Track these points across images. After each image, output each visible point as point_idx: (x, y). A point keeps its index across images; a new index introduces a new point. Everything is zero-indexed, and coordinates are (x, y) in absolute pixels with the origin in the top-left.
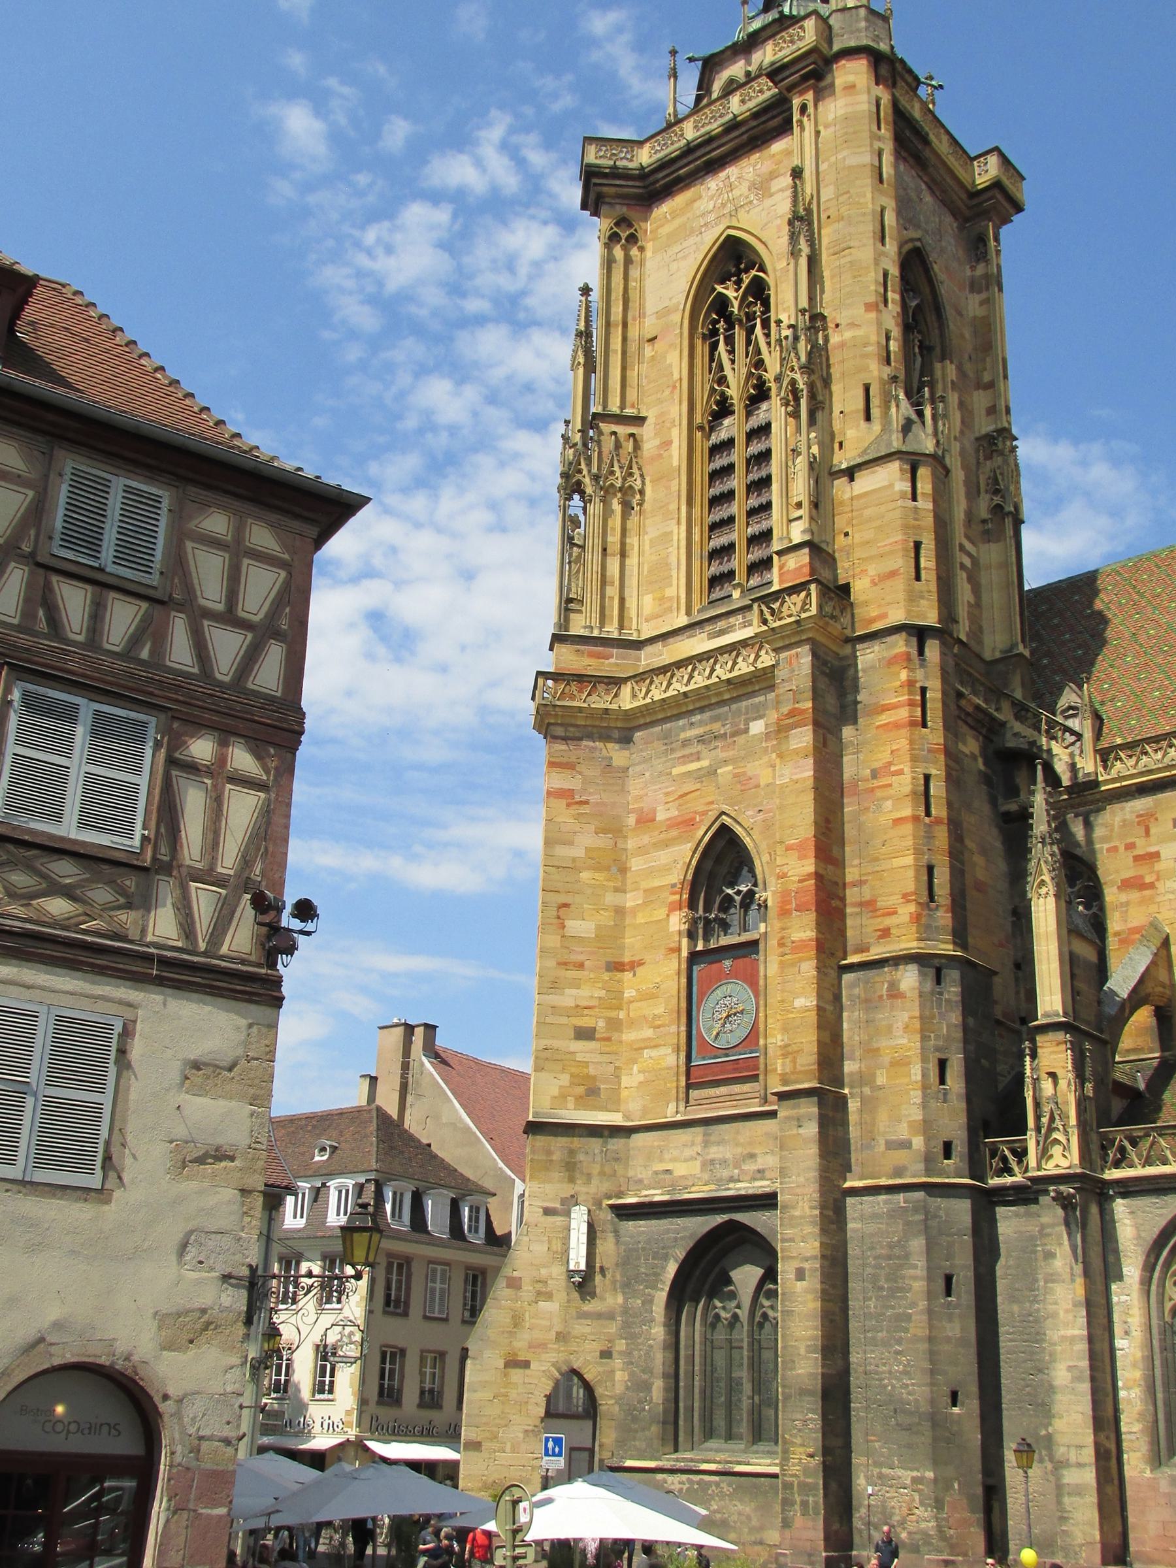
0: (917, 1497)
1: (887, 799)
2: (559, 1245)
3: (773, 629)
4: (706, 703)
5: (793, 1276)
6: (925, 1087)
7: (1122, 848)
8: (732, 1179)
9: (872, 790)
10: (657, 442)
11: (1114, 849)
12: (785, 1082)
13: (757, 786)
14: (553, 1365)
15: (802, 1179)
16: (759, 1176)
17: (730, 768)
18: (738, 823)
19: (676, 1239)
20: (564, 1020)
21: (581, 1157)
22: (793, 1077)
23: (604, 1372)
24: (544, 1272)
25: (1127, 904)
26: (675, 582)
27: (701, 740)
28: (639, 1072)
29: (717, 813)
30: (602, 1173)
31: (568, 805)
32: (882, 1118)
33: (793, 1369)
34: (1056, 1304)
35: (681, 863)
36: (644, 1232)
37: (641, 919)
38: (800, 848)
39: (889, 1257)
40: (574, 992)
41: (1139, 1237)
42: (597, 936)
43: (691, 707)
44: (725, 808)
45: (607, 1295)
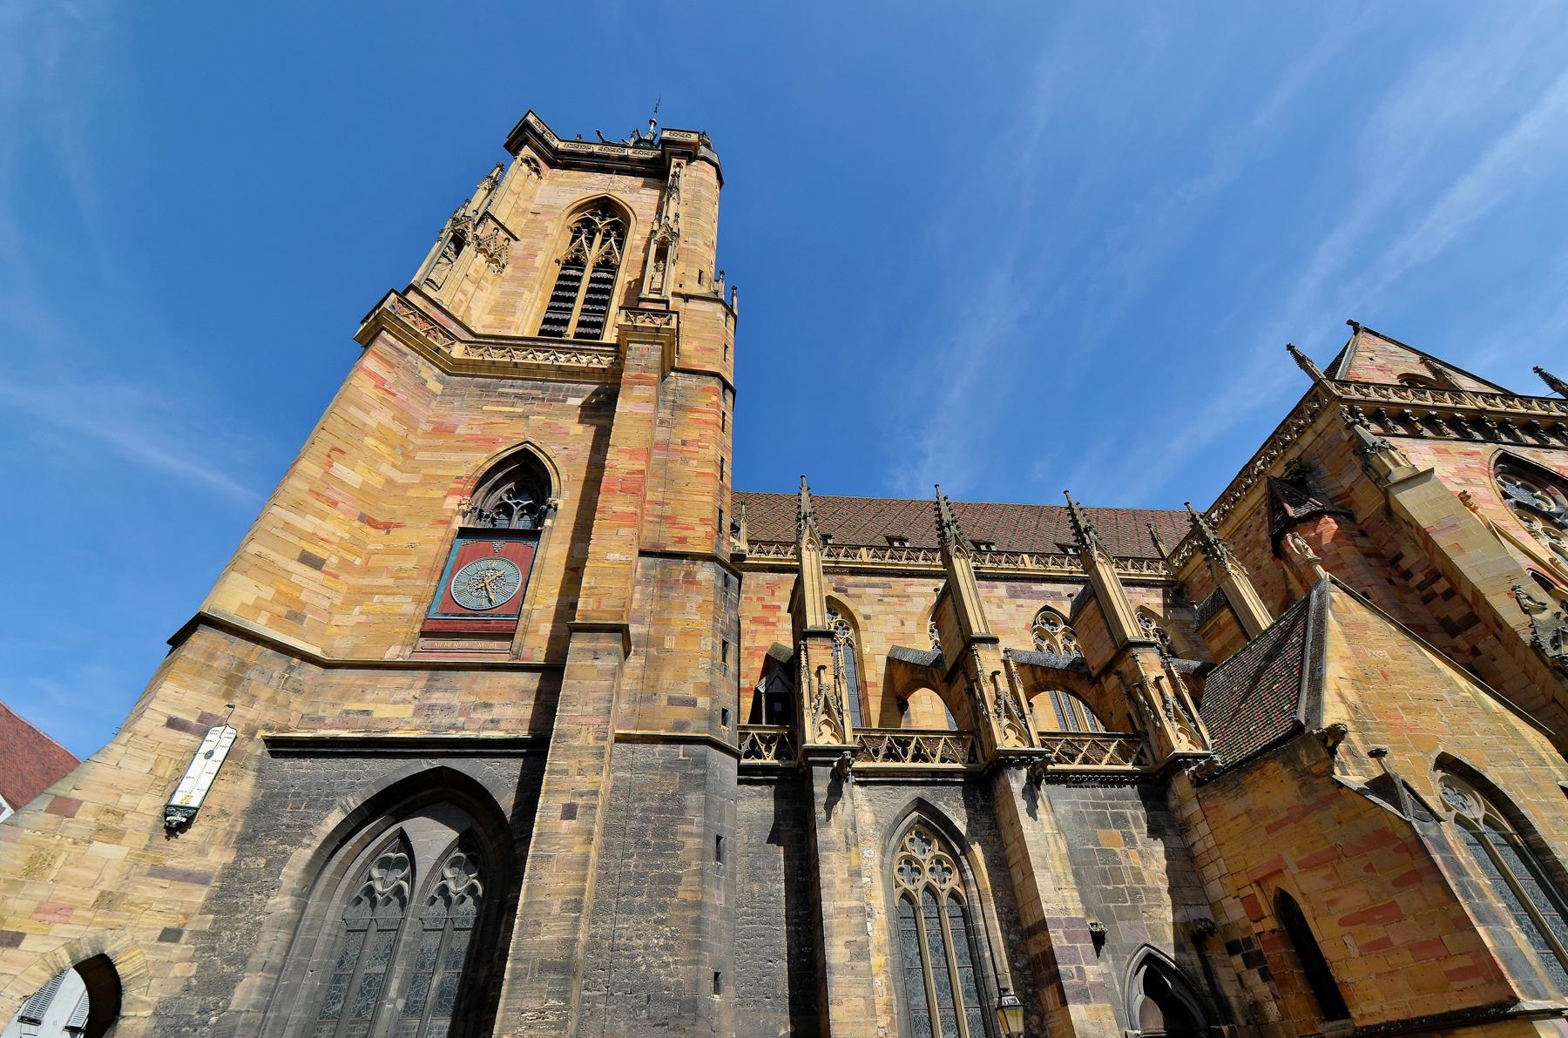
2: (171, 769)
3: (635, 327)
6: (713, 658)
7: (755, 599)
8: (453, 727)
9: (681, 451)
11: (751, 599)
13: (568, 433)
14: (70, 946)
15: (589, 709)
16: (491, 725)
19: (352, 786)
20: (295, 540)
21: (253, 675)
22: (594, 614)
23: (154, 963)
24: (126, 800)
25: (756, 631)
27: (517, 396)
28: (361, 613)
30: (272, 700)
31: (376, 387)
32: (667, 678)
34: (831, 872)
35: (472, 465)
36: (305, 775)
37: (411, 493)
39: (660, 810)
40: (318, 521)
41: (877, 823)
42: (360, 489)
45: (212, 850)
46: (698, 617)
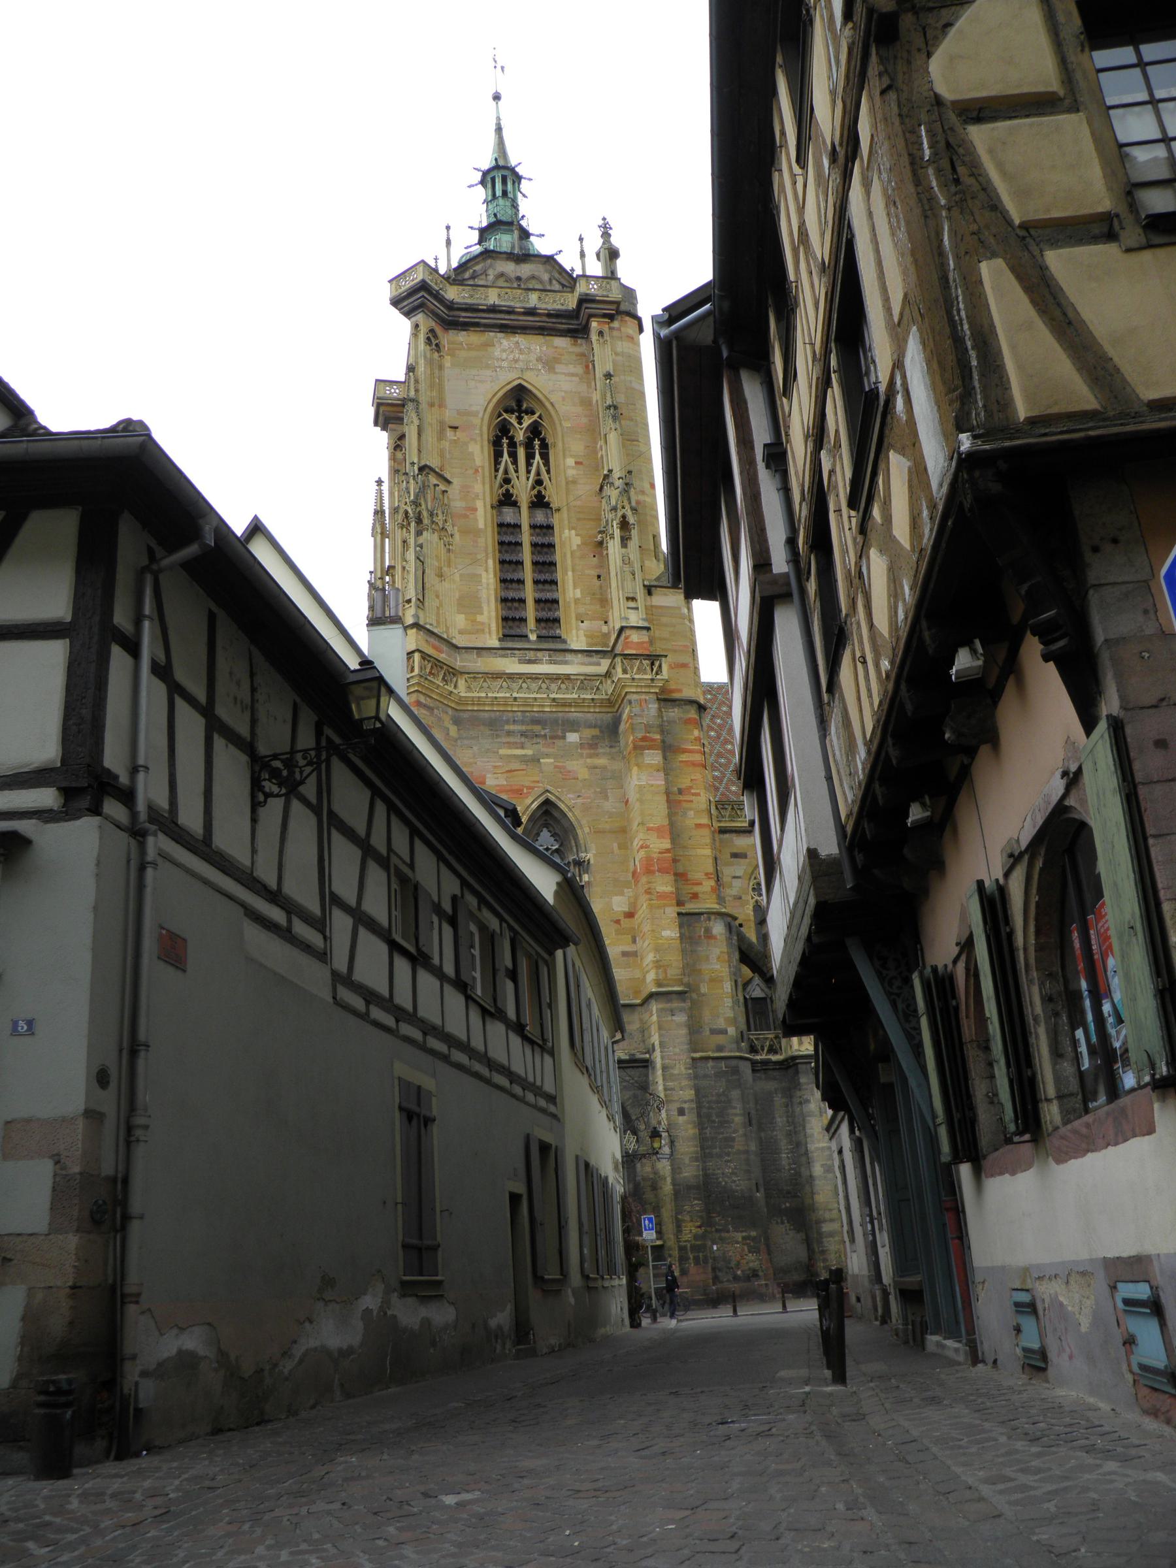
0: (746, 1248)
1: (691, 809)
3: (633, 679)
4: (529, 709)
5: (676, 1113)
9: (680, 802)
10: (463, 504)
12: (659, 985)
15: (677, 1050)
17: (552, 760)
18: (560, 799)
22: (665, 982)
26: (486, 613)
29: (541, 790)
32: (707, 1015)
33: (680, 1173)
38: (659, 830)
39: (718, 1102)
43: (515, 709)
44: (549, 788)
46: (719, 967)
